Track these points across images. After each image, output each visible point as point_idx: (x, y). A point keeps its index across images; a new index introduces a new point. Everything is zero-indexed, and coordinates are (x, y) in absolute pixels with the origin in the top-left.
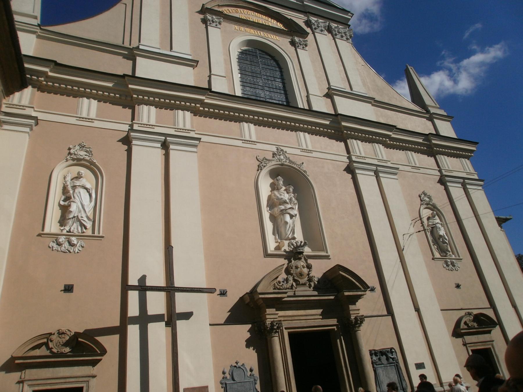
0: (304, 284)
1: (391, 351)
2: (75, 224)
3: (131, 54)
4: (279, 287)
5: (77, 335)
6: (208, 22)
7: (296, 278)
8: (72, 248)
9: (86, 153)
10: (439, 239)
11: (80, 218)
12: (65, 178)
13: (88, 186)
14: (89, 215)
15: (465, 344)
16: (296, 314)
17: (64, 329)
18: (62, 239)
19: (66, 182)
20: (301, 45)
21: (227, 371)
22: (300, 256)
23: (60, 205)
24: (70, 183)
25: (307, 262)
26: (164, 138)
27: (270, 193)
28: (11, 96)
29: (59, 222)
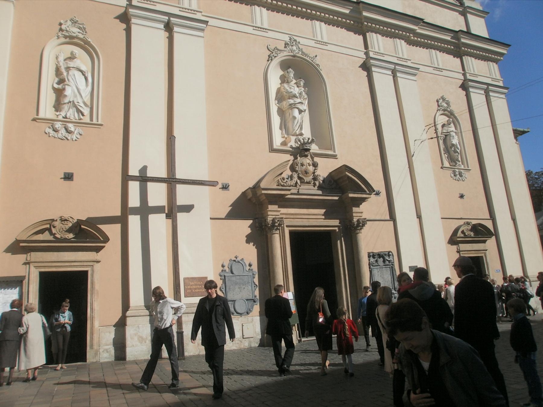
0: (309, 183)
2: (71, 110)
4: (282, 184)
5: (79, 222)
7: (300, 176)
8: (70, 135)
9: (79, 30)
11: (76, 103)
12: (57, 58)
13: (83, 68)
14: (85, 100)
17: (66, 216)
18: (58, 125)
19: (58, 62)
22: (306, 153)
23: (54, 88)
24: (64, 64)
25: (313, 160)
27: (279, 86)
29: (54, 107)
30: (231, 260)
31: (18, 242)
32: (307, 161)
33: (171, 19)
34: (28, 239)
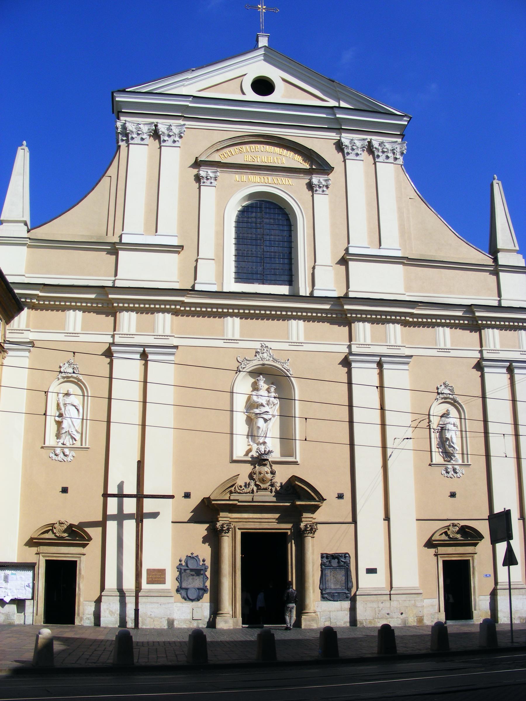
0: (265, 489)
1: (346, 555)
3: (114, 249)
4: (239, 491)
5: (71, 526)
6: (202, 181)
7: (257, 483)
10: (446, 442)
14: (77, 429)
15: (436, 555)
16: (251, 517)
17: (63, 520)
18: (58, 451)
20: (320, 187)
21: (183, 559)
22: (264, 463)
25: (271, 468)
26: (142, 349)
28: (12, 322)
30: (187, 556)
31: (32, 539)
32: (267, 469)
33: (146, 349)
34: (38, 537)
